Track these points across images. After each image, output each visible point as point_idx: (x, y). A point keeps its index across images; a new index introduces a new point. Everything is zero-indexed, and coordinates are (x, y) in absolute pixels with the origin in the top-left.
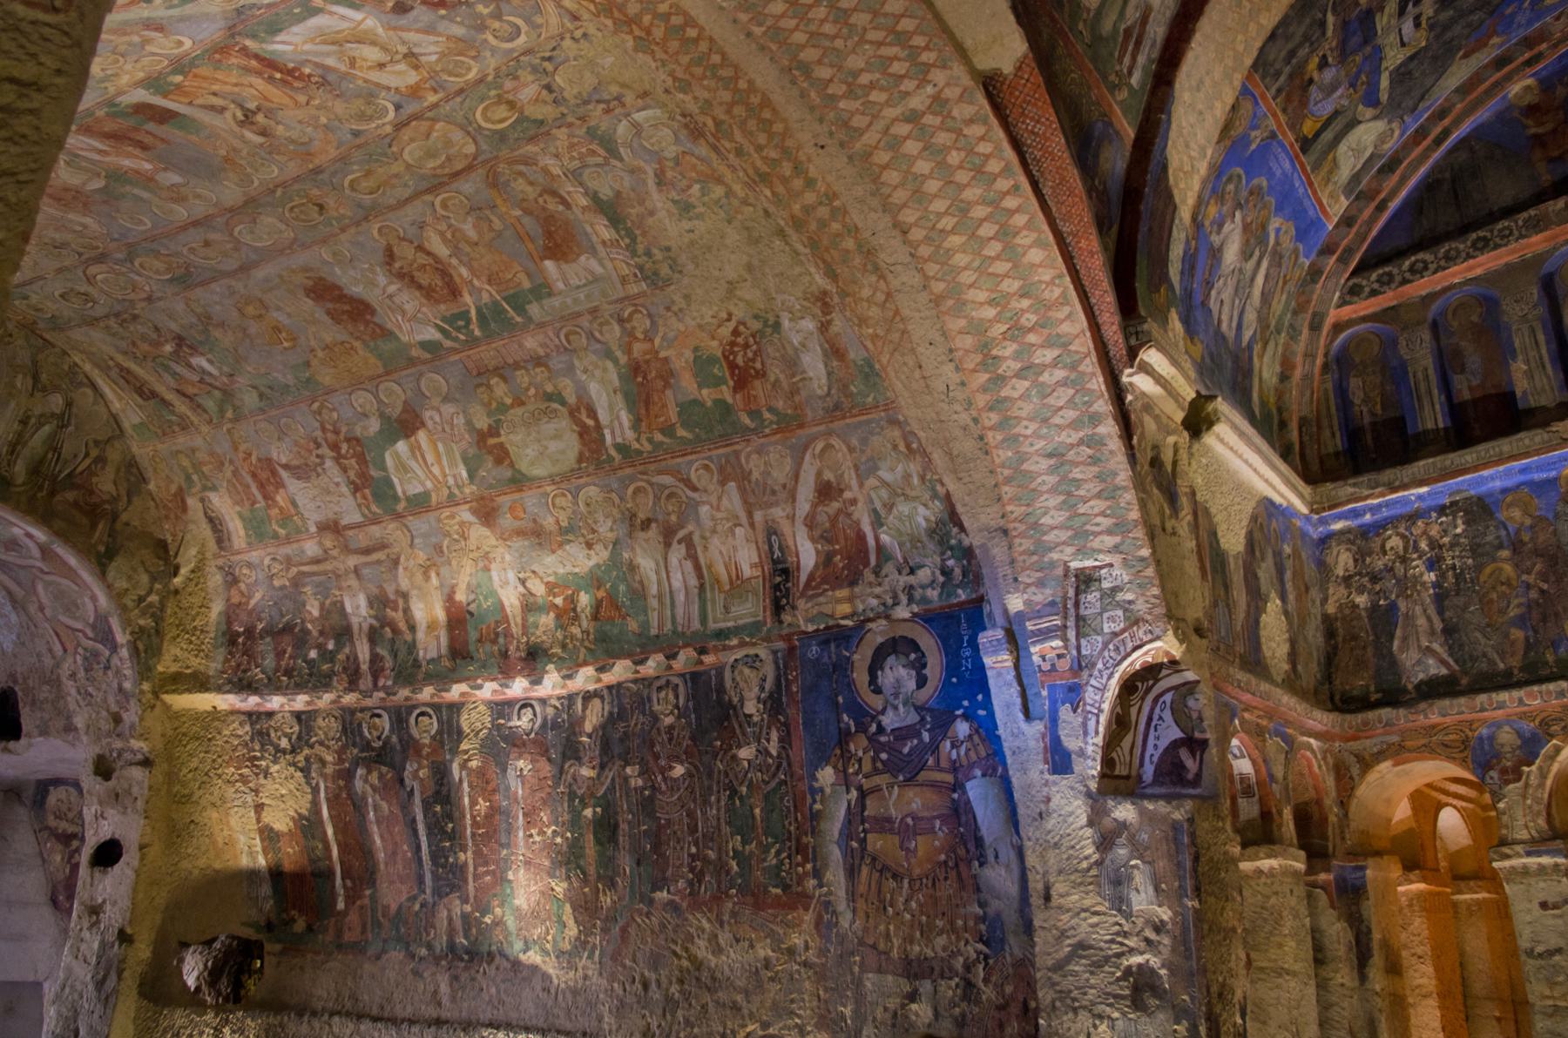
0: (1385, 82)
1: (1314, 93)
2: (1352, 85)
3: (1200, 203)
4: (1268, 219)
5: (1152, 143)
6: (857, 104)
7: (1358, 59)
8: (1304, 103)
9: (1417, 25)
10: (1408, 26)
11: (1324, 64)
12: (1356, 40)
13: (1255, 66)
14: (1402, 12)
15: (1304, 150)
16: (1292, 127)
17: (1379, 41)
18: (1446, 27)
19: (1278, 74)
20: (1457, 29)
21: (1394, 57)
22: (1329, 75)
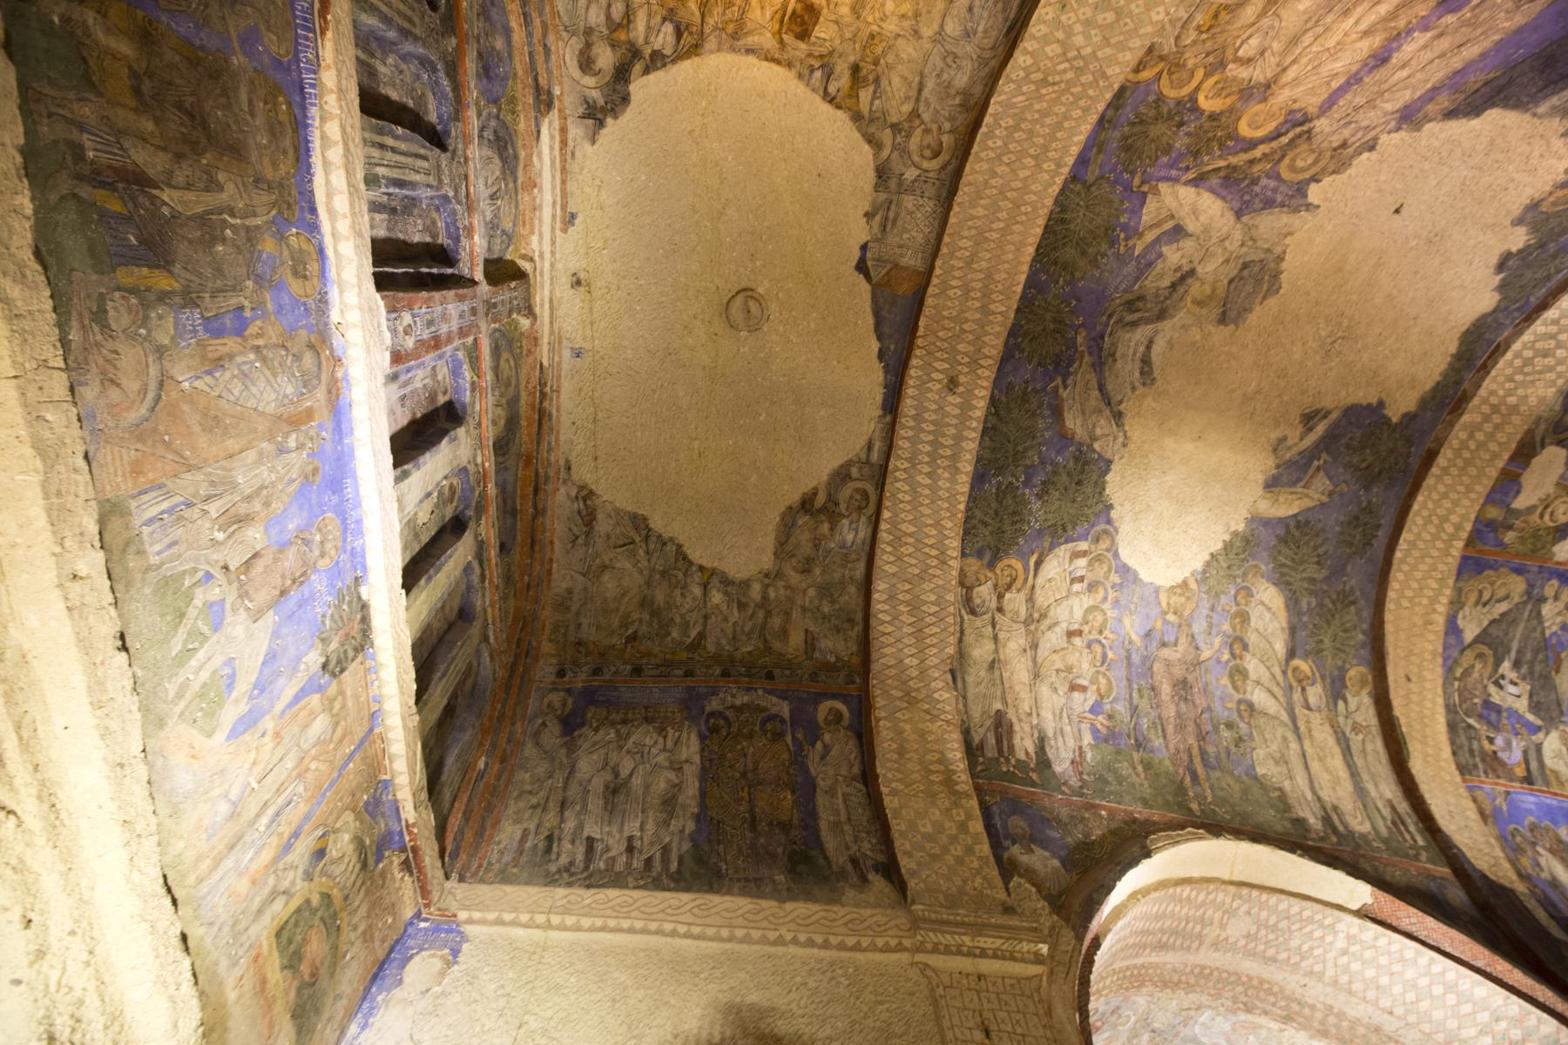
0: (1531, 717)
1: (1503, 755)
2: (1517, 734)
3: (1513, 863)
4: (1557, 835)
5: (1465, 870)
6: (1310, 961)
7: (1505, 721)
8: (1503, 764)
9: (1515, 684)
10: (1512, 689)
11: (1491, 740)
12: (1493, 717)
13: (1462, 774)
14: (1501, 687)
15: (1531, 783)
16: (1512, 780)
17: (1505, 706)
18: (1531, 672)
19: (1476, 766)
20: (1538, 668)
21: (1522, 705)
22: (1499, 741)
